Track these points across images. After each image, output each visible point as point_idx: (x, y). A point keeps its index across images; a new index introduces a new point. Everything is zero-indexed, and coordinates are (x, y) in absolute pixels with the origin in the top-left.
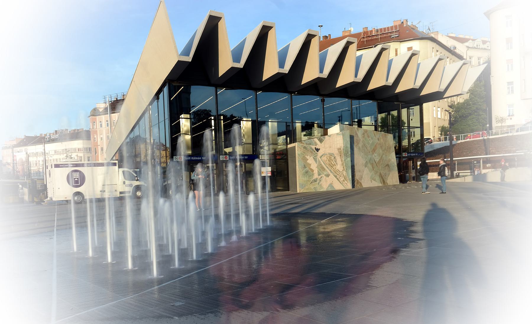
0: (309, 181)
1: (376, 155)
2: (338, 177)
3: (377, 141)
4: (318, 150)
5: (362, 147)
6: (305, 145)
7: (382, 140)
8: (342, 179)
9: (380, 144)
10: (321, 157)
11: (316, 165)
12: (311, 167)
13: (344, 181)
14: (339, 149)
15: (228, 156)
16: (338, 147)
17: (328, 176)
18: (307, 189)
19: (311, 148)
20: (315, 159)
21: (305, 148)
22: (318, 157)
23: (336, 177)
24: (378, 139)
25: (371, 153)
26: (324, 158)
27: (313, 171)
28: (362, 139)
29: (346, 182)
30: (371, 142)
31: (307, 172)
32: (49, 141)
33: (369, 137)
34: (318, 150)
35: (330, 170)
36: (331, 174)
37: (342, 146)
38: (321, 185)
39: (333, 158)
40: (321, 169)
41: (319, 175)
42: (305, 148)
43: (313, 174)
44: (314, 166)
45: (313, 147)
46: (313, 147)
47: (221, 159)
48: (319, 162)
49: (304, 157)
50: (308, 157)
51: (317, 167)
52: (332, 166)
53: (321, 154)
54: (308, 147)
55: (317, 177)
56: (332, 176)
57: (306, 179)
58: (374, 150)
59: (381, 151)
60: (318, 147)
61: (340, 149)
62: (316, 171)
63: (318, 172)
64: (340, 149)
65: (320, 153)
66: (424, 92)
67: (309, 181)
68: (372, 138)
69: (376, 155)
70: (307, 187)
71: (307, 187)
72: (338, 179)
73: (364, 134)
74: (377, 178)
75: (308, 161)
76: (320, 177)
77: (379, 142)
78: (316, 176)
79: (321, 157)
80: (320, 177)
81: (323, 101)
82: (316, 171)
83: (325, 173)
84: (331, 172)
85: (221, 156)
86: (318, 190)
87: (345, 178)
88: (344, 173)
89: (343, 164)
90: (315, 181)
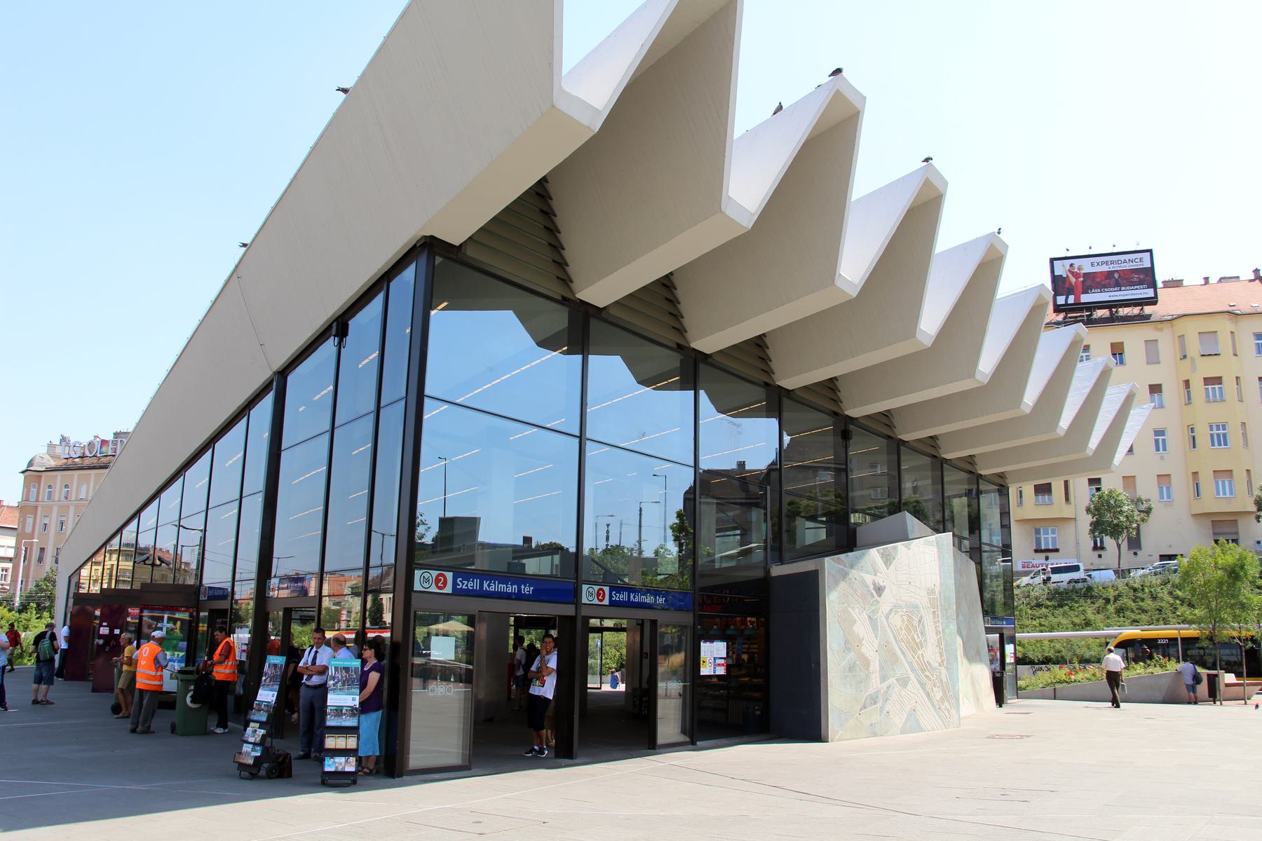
2: (928, 687)
4: (879, 590)
8: (938, 694)
10: (887, 617)
11: (876, 644)
12: (864, 650)
13: (942, 700)
17: (904, 682)
19: (863, 582)
23: (923, 685)
27: (866, 663)
29: (946, 704)
31: (851, 668)
34: (879, 590)
35: (910, 664)
40: (889, 659)
41: (883, 679)
44: (870, 648)
46: (869, 579)
50: (855, 613)
52: (916, 646)
56: (913, 685)
62: (875, 665)
63: (882, 668)
72: (928, 694)
78: (875, 683)
82: (875, 665)
84: (913, 670)
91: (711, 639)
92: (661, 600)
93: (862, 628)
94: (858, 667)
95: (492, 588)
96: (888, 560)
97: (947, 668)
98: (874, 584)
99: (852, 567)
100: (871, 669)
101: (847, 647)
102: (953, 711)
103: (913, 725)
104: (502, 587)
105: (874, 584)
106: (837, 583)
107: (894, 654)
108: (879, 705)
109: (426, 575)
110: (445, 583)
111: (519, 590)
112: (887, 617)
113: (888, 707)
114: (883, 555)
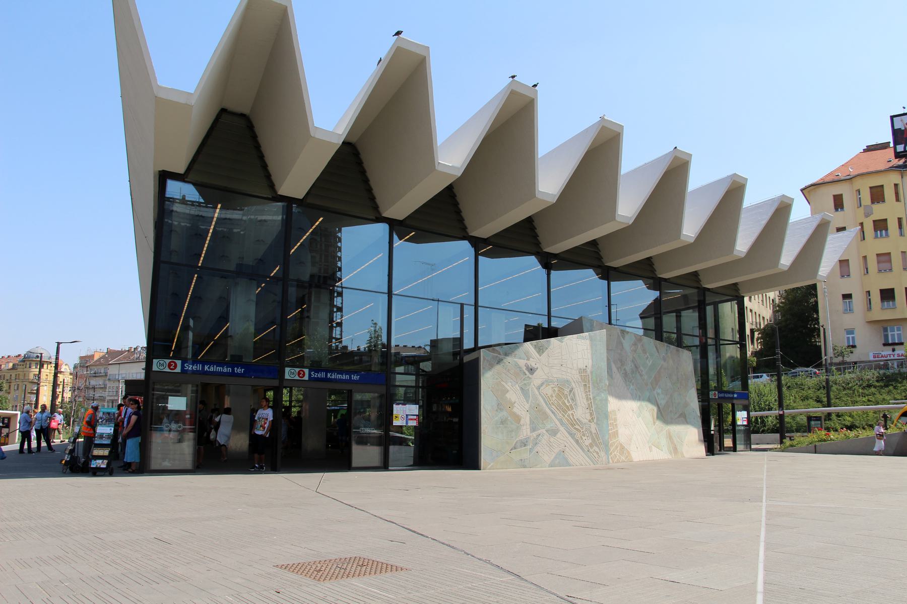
2: (578, 436)
4: (532, 370)
11: (527, 406)
12: (515, 410)
14: (582, 371)
15: (306, 371)
16: (582, 366)
17: (554, 432)
20: (524, 391)
26: (548, 390)
27: (518, 419)
29: (595, 448)
30: (649, 363)
31: (503, 422)
33: (644, 351)
34: (532, 370)
36: (562, 428)
39: (566, 391)
40: (539, 416)
41: (533, 430)
44: (522, 409)
46: (522, 363)
47: (287, 377)
50: (508, 386)
52: (565, 409)
55: (529, 433)
56: (563, 433)
60: (532, 363)
63: (532, 422)
65: (537, 379)
69: (660, 391)
72: (577, 442)
73: (635, 344)
74: (664, 442)
75: (508, 395)
76: (535, 434)
79: (538, 388)
80: (535, 434)
82: (526, 419)
83: (548, 426)
84: (562, 424)
85: (287, 370)
87: (593, 440)
88: (593, 426)
89: (589, 407)
91: (407, 401)
92: (355, 377)
93: (513, 394)
94: (510, 422)
95: (212, 369)
96: (540, 350)
97: (597, 424)
99: (506, 355)
100: (522, 422)
101: (499, 407)
102: (602, 454)
103: (561, 460)
104: (219, 369)
106: (491, 366)
107: (545, 413)
108: (528, 447)
109: (162, 362)
110: (176, 366)
111: (233, 370)
112: (538, 388)
113: (538, 448)
114: (535, 347)
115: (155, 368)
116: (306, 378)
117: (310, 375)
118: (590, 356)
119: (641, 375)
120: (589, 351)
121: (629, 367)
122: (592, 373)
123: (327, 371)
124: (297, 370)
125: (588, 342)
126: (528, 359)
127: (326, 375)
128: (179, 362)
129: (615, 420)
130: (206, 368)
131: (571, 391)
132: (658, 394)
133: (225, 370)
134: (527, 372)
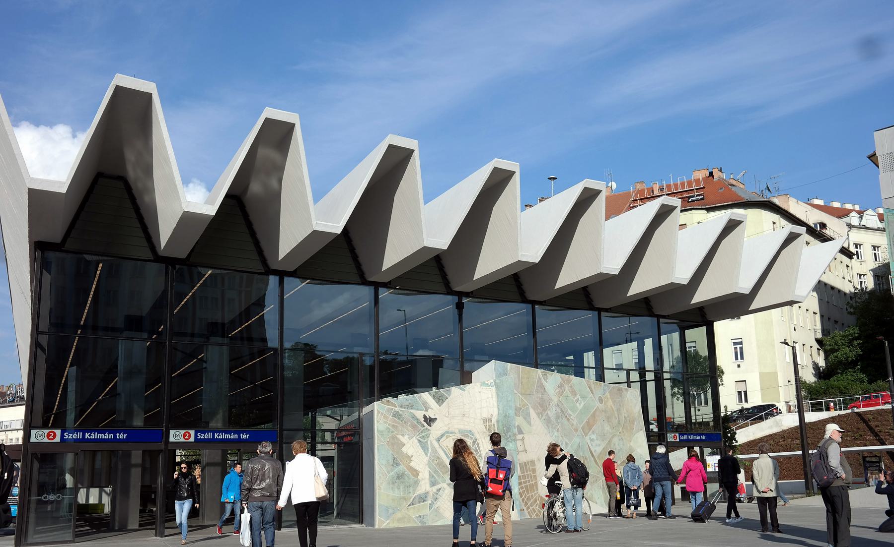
0: (405, 499)
1: (594, 437)
3: (598, 404)
4: (429, 421)
5: (557, 417)
6: (398, 409)
7: (610, 403)
9: (605, 411)
10: (438, 440)
11: (425, 459)
12: (412, 464)
16: (485, 415)
18: (399, 520)
19: (414, 417)
20: (424, 446)
21: (396, 415)
22: (432, 438)
24: (601, 400)
25: (580, 431)
27: (416, 473)
28: (555, 400)
30: (580, 406)
31: (400, 476)
32: (13, 401)
33: (574, 393)
34: (429, 421)
37: (495, 412)
38: (437, 510)
41: (433, 484)
42: (396, 415)
43: (417, 483)
45: (420, 414)
47: (172, 439)
48: (434, 451)
49: (394, 438)
50: (404, 439)
51: (429, 464)
53: (439, 433)
54: (406, 413)
57: (397, 493)
58: (589, 426)
59: (607, 428)
60: (430, 414)
61: (490, 420)
63: (431, 476)
64: (490, 420)
65: (436, 429)
66: (701, 296)
67: (405, 499)
68: (584, 397)
69: (594, 437)
70: (399, 515)
71: (399, 515)
73: (561, 386)
75: (404, 449)
76: (434, 489)
77: (601, 406)
79: (438, 440)
80: (434, 489)
81: (460, 306)
85: (172, 432)
86: (430, 523)
90: (423, 499)
93: (410, 446)
95: (93, 437)
96: (440, 400)
98: (425, 417)
100: (420, 477)
104: (101, 436)
105: (425, 417)
108: (429, 502)
109: (40, 433)
111: (115, 436)
115: (33, 439)
116: (192, 439)
117: (196, 436)
118: (495, 404)
119: (568, 420)
120: (495, 399)
121: (552, 412)
122: (498, 421)
123: (214, 432)
124: (183, 432)
125: (494, 388)
126: (427, 410)
127: (213, 436)
128: (58, 432)
129: (534, 471)
130: (87, 435)
131: (474, 442)
132: (592, 440)
133: (107, 436)
134: (425, 424)
